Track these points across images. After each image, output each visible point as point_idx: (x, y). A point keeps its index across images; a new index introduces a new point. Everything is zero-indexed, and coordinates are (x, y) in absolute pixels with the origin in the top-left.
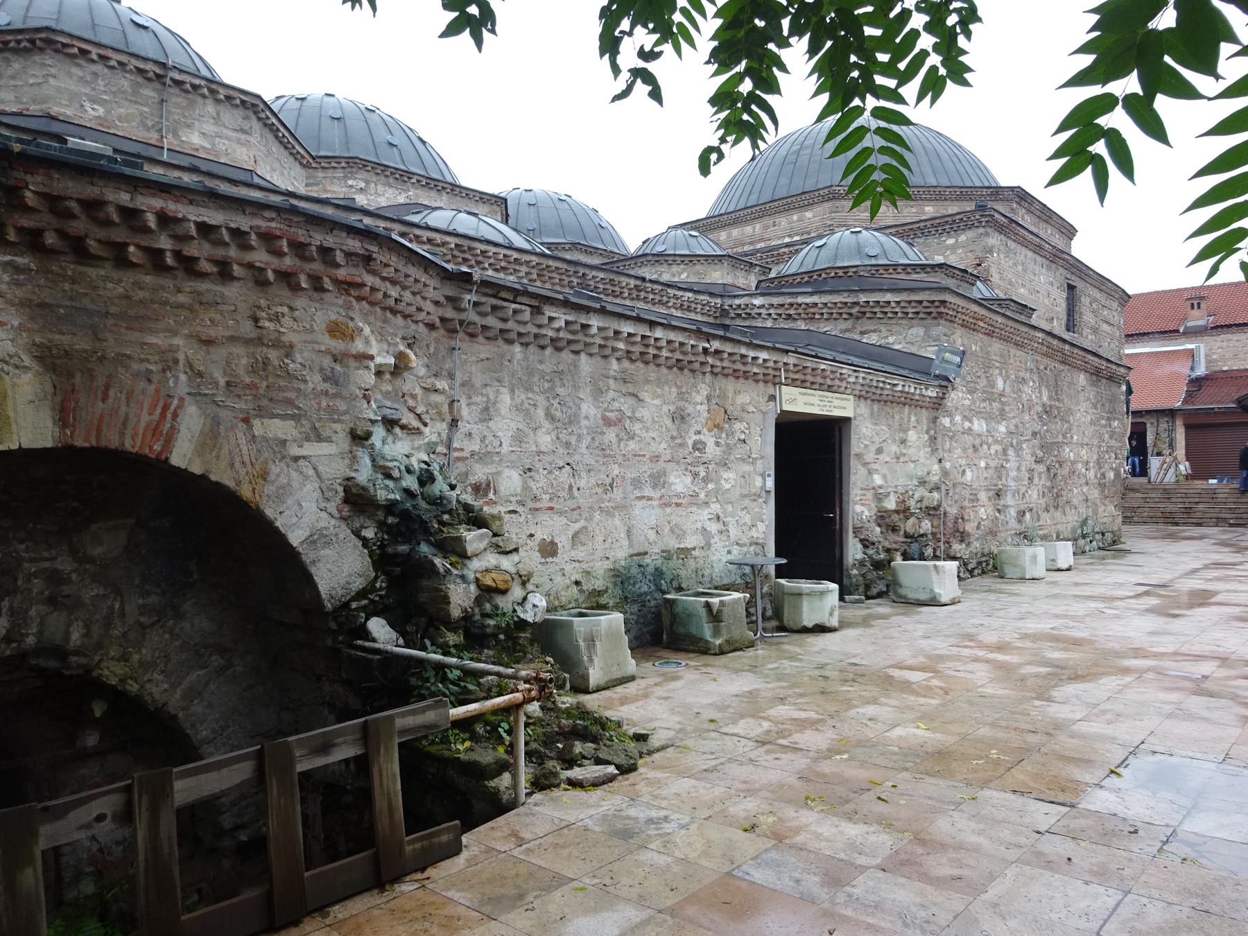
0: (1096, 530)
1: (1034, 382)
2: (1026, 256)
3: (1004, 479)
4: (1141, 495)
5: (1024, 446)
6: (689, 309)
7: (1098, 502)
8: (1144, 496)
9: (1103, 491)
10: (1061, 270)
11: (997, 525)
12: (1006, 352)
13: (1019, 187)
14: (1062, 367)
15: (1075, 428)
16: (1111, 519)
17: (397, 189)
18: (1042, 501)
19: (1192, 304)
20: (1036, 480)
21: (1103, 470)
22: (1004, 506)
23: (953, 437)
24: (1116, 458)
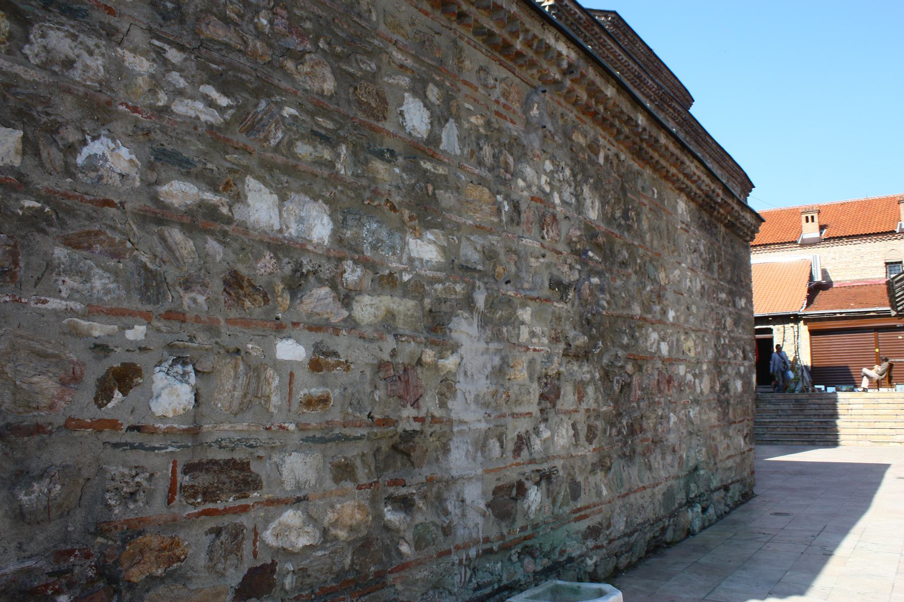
0: (715, 483)
1: (553, 159)
3: (430, 405)
4: (773, 407)
5: (526, 314)
7: (717, 434)
8: (777, 407)
9: (725, 414)
11: (391, 550)
12: (442, 41)
13: (615, 13)
15: (670, 296)
16: (738, 460)
18: (587, 451)
19: (807, 218)
20: (568, 398)
21: (725, 377)
22: (430, 481)
23: (34, 220)
24: (745, 358)
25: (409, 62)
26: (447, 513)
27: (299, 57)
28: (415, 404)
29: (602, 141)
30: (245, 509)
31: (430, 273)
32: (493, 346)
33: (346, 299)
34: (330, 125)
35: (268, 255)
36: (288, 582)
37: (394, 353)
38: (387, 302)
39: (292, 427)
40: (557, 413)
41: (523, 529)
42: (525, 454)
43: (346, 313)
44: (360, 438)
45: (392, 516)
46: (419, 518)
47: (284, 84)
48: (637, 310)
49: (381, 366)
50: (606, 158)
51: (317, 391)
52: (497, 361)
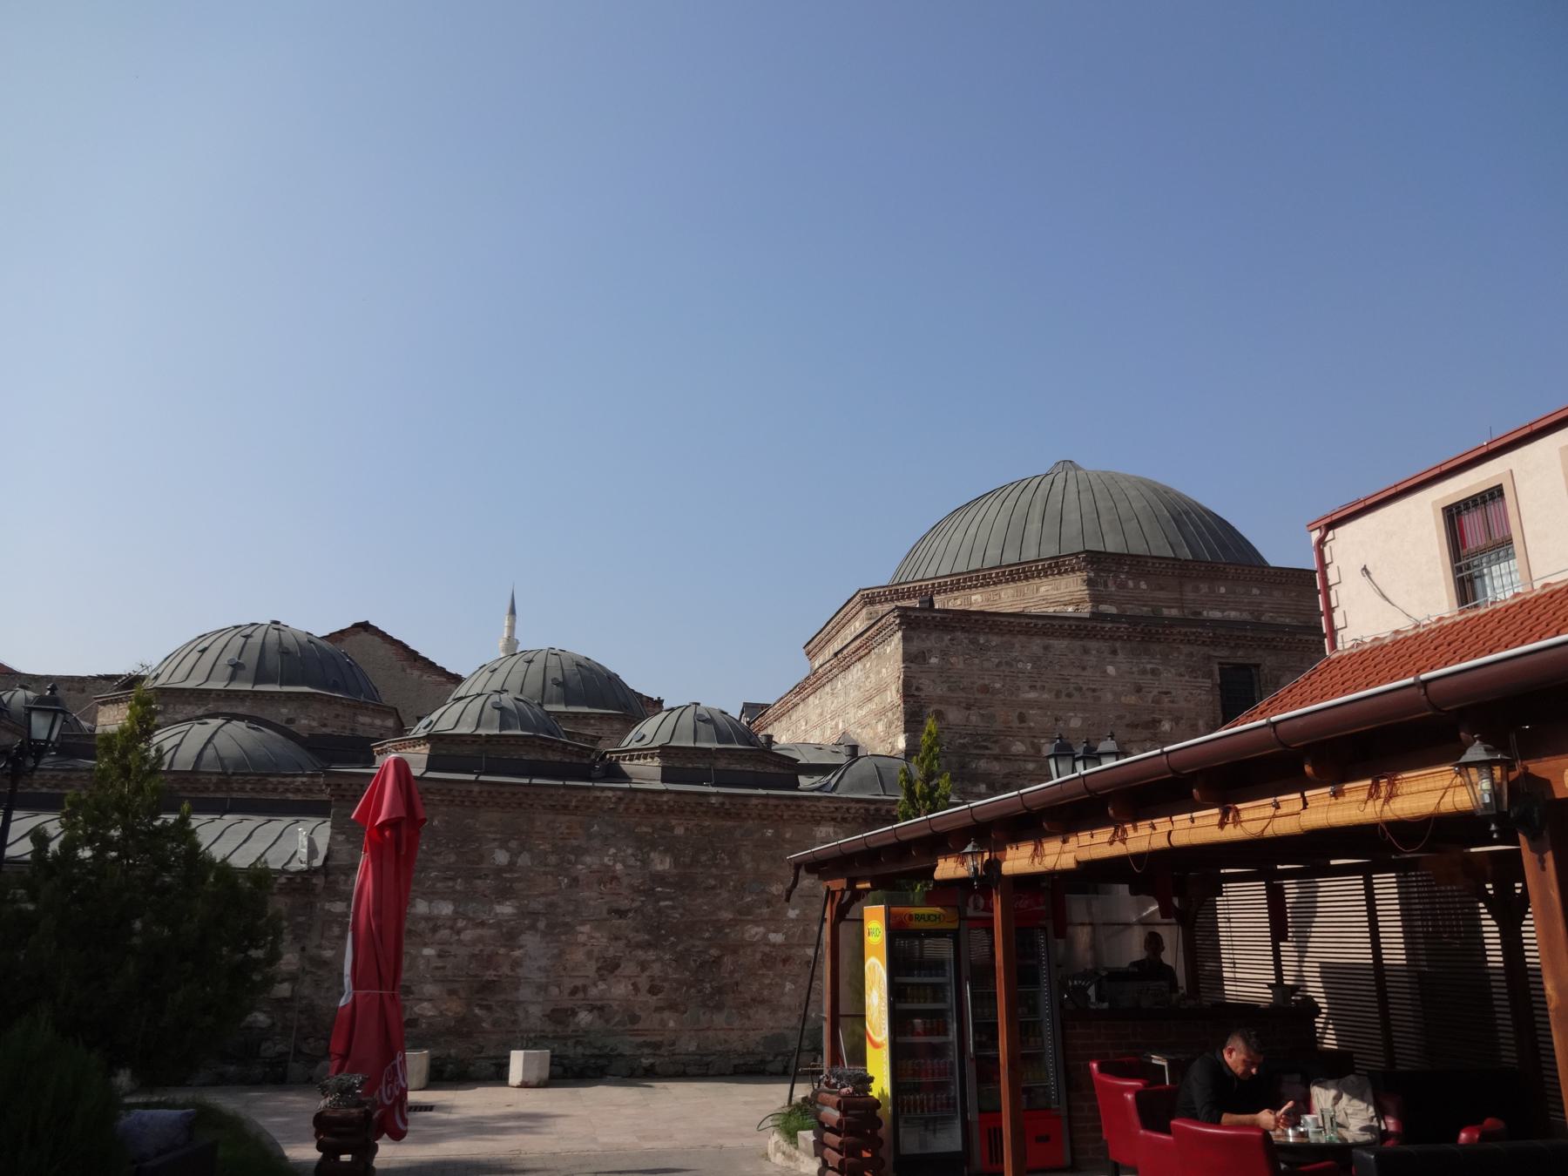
2: (1046, 648)
6: (310, 791)
10: (1186, 649)
14: (730, 824)
17: (196, 704)
20: (629, 968)
25: (498, 836)
26: (516, 1015)
27: (438, 854)
28: (495, 970)
29: (674, 822)
30: (408, 1000)
31: (507, 918)
32: (551, 945)
33: (458, 932)
34: (452, 873)
35: (423, 922)
36: (424, 1026)
37: (481, 951)
38: (479, 931)
39: (428, 976)
40: (616, 976)
41: (573, 1031)
42: (580, 995)
43: (457, 938)
44: (462, 981)
45: (477, 1011)
46: (497, 1015)
47: (432, 865)
48: (726, 915)
49: (473, 956)
50: (687, 829)
51: (440, 965)
52: (556, 951)
